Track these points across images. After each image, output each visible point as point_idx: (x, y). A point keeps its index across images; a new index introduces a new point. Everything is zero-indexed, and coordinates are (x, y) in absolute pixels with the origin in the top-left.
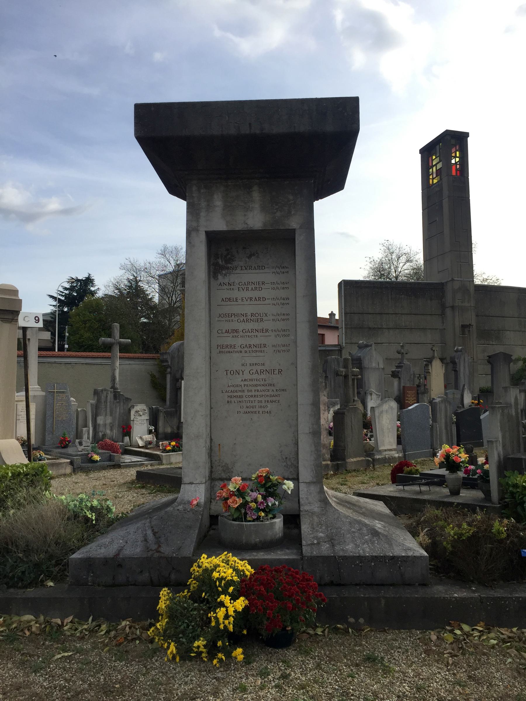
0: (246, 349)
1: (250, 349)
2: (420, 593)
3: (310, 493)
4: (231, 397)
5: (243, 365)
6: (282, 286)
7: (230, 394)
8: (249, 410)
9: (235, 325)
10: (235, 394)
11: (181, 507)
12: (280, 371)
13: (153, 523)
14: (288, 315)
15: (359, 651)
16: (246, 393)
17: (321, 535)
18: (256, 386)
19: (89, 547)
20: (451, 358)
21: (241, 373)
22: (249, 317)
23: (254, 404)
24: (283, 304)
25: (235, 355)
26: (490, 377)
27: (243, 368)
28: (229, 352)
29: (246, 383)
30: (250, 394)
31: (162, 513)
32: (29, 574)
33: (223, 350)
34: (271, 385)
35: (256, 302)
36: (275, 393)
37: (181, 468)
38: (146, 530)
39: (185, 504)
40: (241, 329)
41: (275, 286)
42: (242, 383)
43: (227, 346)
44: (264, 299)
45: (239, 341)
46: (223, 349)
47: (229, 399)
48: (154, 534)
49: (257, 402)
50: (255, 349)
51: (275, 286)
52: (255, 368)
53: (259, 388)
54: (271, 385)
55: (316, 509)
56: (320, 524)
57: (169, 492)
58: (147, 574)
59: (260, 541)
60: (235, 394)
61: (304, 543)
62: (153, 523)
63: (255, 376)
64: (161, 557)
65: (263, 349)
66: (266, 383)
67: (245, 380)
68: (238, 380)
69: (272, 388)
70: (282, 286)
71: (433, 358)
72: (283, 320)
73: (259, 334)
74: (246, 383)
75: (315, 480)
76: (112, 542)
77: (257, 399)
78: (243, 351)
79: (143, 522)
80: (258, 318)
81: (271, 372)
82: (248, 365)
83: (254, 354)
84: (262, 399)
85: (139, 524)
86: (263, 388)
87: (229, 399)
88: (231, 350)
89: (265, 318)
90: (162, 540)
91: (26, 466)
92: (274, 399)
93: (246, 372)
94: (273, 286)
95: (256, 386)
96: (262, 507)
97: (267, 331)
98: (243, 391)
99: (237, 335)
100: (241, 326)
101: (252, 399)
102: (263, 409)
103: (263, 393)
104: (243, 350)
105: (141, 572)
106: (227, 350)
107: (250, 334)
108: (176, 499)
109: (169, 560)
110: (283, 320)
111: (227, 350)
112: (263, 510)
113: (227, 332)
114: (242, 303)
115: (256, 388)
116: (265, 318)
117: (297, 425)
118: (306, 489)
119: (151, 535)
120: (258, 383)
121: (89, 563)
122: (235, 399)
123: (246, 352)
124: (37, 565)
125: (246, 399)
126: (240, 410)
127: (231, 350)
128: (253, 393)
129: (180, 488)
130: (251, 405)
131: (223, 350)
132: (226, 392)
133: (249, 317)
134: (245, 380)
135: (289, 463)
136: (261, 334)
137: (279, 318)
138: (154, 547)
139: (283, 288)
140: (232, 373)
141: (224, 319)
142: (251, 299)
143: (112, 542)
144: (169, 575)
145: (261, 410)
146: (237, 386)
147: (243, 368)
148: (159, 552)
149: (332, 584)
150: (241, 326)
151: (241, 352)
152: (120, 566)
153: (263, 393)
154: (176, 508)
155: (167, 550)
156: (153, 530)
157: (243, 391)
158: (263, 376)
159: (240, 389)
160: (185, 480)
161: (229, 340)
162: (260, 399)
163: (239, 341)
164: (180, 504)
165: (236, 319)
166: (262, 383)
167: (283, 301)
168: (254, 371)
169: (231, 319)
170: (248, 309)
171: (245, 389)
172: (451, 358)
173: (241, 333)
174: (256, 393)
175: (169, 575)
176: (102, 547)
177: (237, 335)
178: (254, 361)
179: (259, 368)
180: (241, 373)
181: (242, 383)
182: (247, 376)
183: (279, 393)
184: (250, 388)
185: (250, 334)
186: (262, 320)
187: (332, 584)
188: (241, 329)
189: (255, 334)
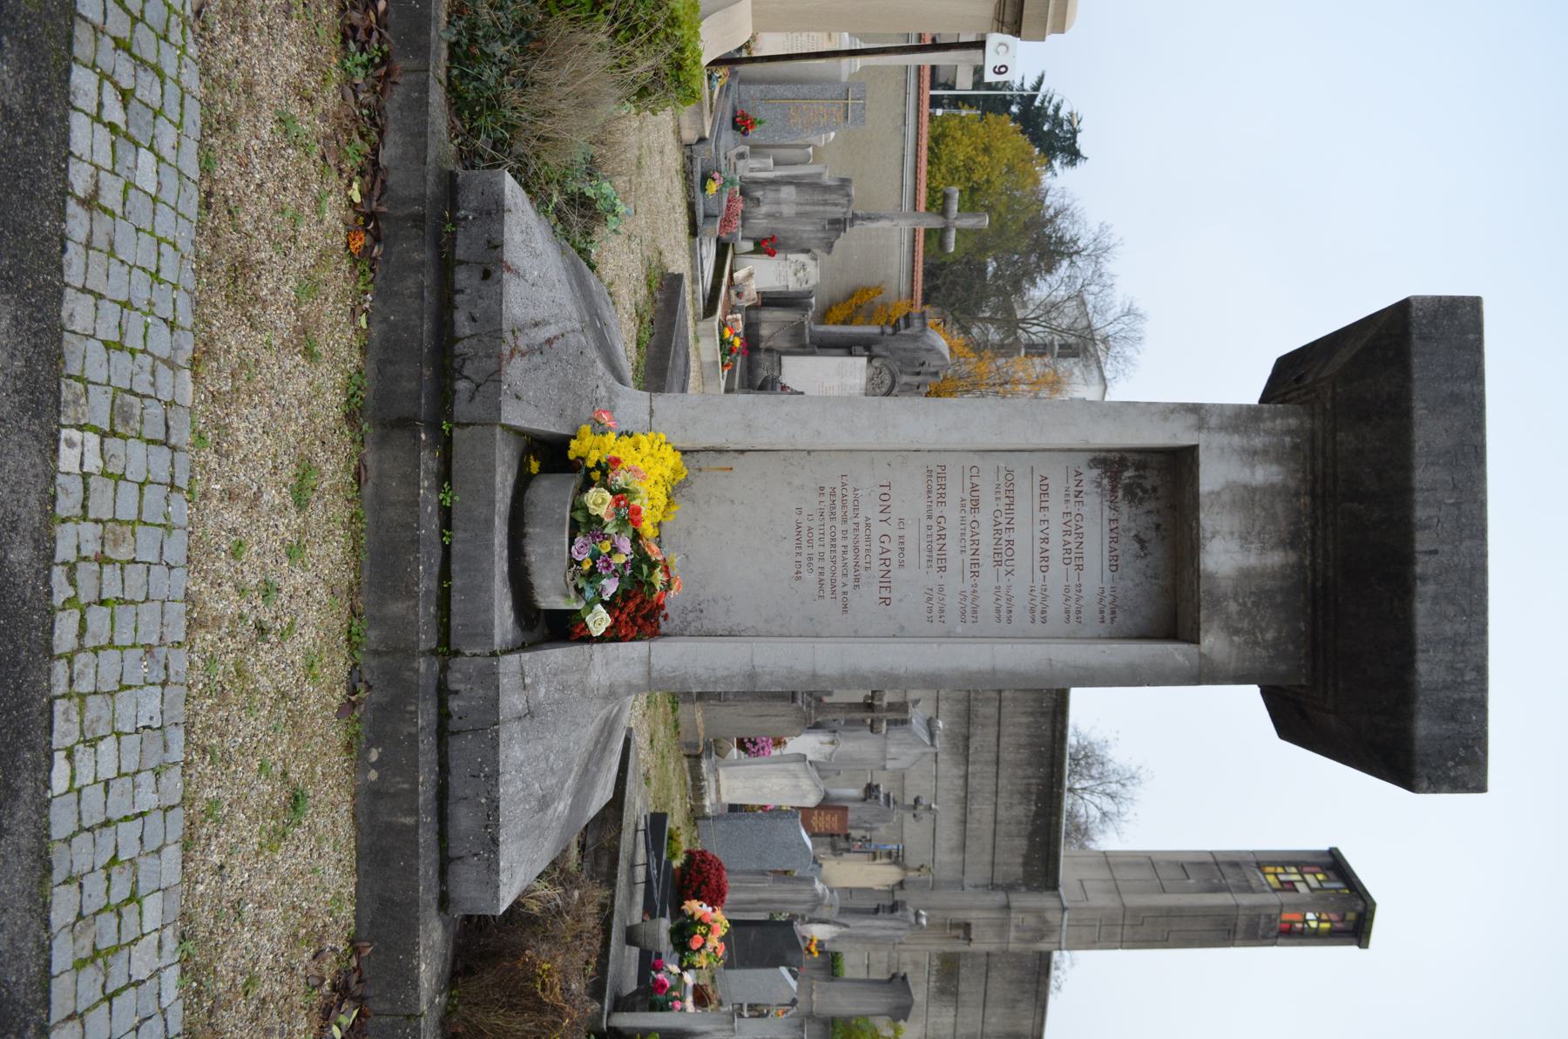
0: (936, 528)
1: (935, 537)
2: (427, 893)
3: (627, 665)
4: (833, 494)
6: (1073, 610)
7: (838, 492)
8: (804, 532)
9: (988, 503)
10: (838, 504)
11: (602, 392)
12: (885, 601)
13: (570, 336)
14: (1009, 620)
15: (314, 773)
16: (840, 527)
17: (542, 691)
18: (856, 548)
19: (528, 207)
20: (903, 903)
21: (884, 517)
22: (1005, 536)
23: (816, 543)
24: (1032, 610)
25: (922, 505)
26: (863, 976)
27: (894, 521)
28: (929, 492)
29: (862, 527)
30: (839, 535)
31: (593, 353)
32: (475, 88)
33: (934, 479)
34: (857, 579)
35: (1037, 551)
36: (839, 590)
37: (684, 390)
38: (557, 322)
39: (610, 399)
40: (978, 517)
41: (1072, 594)
42: (861, 520)
43: (942, 486)
45: (952, 514)
47: (827, 491)
48: (549, 342)
49: (822, 549)
50: (936, 547)
51: (1072, 594)
52: (894, 546)
53: (850, 555)
54: (857, 579)
55: (594, 677)
56: (564, 687)
57: (636, 370)
58: (468, 332)
59: (530, 564)
60: (838, 504)
61: (526, 656)
62: (570, 336)
63: (876, 548)
64: (499, 356)
65: (935, 564)
66: (862, 571)
67: (868, 526)
68: (869, 509)
69: (851, 584)
70: (1073, 610)
71: (905, 868)
72: (998, 611)
73: (967, 557)
74: (862, 527)
75: (654, 675)
76: (536, 255)
77: (827, 549)
78: (930, 522)
79: (575, 315)
80: (1003, 555)
81: (885, 583)
82: (901, 533)
83: (924, 545)
84: (827, 564)
85: (570, 308)
86: (851, 563)
87: (827, 491)
88: (934, 496)
90: (537, 359)
91: (696, 63)
92: (827, 587)
93: (885, 528)
94: (1073, 589)
95: (856, 548)
96: (600, 564)
97: (975, 574)
98: (845, 521)
99: (967, 508)
100: (985, 517)
101: (827, 539)
102: (805, 562)
103: (839, 564)
104: (932, 522)
105: (474, 319)
106: (935, 487)
107: (968, 537)
108: (621, 381)
109: (495, 376)
110: (998, 611)
111: (935, 487)
112: (593, 570)
113: (974, 488)
114: (1037, 520)
115: (850, 549)
116: (1002, 569)
117: (769, 635)
118: (635, 655)
119: (548, 335)
120: (862, 553)
121: (495, 210)
122: (827, 498)
123: (929, 528)
124: (493, 105)
125: (827, 527)
126: (805, 513)
127: (934, 496)
128: (839, 543)
129: (645, 389)
130: (816, 537)
131: (934, 479)
132: (844, 484)
133: (1005, 536)
134: (868, 526)
135: (691, 617)
136: (968, 562)
137: (1003, 602)
138: (522, 343)
139: (1067, 612)
141: (1002, 478)
142: (1045, 540)
143: (536, 255)
144: (467, 378)
145: (804, 559)
146: (856, 508)
147: (894, 521)
148: (512, 355)
149: (444, 715)
150: (985, 517)
151: (930, 517)
152: (486, 275)
153: (839, 564)
154: (600, 383)
155: (514, 371)
156: (556, 337)
157: (845, 521)
158: (876, 563)
159: (850, 514)
160: (660, 400)
161: (954, 493)
162: (827, 556)
163: (952, 514)
164: (609, 389)
165: (1002, 508)
166: (862, 562)
167: (1038, 609)
168: (886, 546)
169: (1002, 495)
170: (1023, 535)
171: (850, 526)
172: (903, 903)
173: (970, 518)
174: (839, 549)
175: (467, 378)
176: (526, 233)
177: (967, 508)
178: (910, 546)
179: (894, 556)
181: (861, 520)
182: (878, 529)
183: (840, 597)
184: (850, 536)
185: (968, 537)
186: (998, 563)
187: (444, 715)
188: (978, 517)
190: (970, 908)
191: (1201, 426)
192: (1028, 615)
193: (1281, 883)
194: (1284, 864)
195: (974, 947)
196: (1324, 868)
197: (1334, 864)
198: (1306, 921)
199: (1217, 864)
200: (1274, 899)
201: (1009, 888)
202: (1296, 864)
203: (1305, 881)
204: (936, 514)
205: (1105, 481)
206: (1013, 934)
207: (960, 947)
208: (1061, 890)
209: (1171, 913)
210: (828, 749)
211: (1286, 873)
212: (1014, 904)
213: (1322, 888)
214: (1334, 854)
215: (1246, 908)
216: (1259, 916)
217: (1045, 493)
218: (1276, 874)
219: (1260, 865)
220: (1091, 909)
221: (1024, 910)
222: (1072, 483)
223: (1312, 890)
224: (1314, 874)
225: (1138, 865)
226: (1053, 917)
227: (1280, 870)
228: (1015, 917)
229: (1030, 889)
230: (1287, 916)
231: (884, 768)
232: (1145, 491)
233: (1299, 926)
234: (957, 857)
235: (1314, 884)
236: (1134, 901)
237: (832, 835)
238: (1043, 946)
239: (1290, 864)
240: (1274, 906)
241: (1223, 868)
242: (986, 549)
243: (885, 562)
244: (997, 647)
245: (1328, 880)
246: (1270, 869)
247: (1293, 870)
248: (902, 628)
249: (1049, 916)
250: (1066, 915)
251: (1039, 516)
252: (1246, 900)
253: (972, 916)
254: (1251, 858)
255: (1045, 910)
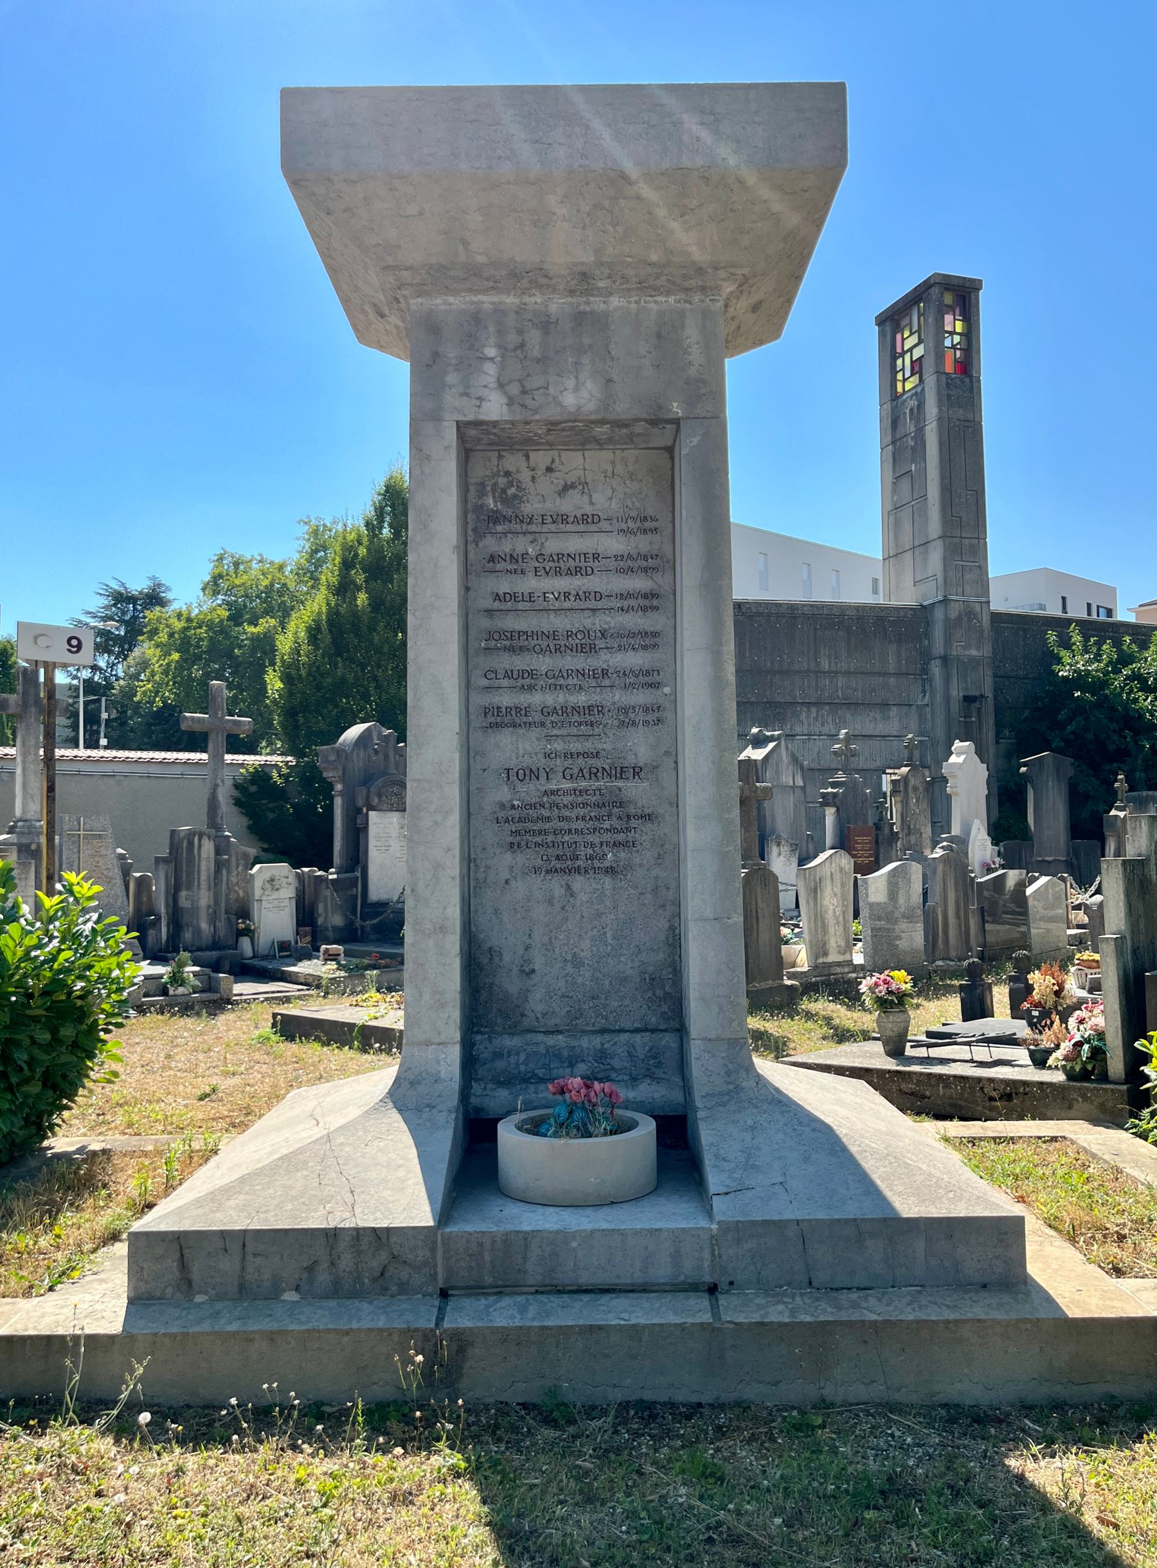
0: (554, 718)
5: (547, 755)
10: (530, 826)
21: (543, 775)
44: (599, 596)
46: (499, 719)
67: (553, 792)
89: (600, 644)
92: (621, 837)
98: (549, 819)
116: (600, 644)
132: (507, 821)
140: (521, 776)
142: (567, 595)
150: (543, 663)
151: (543, 724)
157: (549, 819)
168: (576, 771)
178: (576, 746)
180: (543, 775)
188: (544, 669)
189: (575, 681)
190: (947, 698)
191: (435, 417)
192: (649, 614)
193: (912, 374)
194: (894, 372)
195: (989, 694)
196: (897, 328)
197: (892, 321)
198: (953, 347)
199: (894, 442)
200: (931, 380)
201: (926, 657)
202: (894, 357)
203: (911, 350)
204: (538, 717)
205: (499, 528)
206: (974, 652)
207: (989, 706)
208: (925, 603)
209: (947, 490)
210: (785, 849)
211: (903, 369)
212: (942, 653)
213: (919, 331)
214: (881, 321)
215: (940, 410)
216: (949, 396)
217: (514, 597)
218: (905, 380)
219: (895, 397)
220: (945, 570)
221: (948, 641)
222: (501, 566)
223: (920, 342)
224: (903, 340)
225: (897, 524)
226: (954, 611)
227: (900, 376)
228: (957, 650)
229: (927, 635)
230: (949, 368)
231: (803, 788)
232: (510, 484)
233: (958, 353)
234: (894, 711)
235: (914, 339)
236: (934, 526)
237: (877, 842)
238: (986, 620)
239: (894, 365)
240: (938, 380)
241: (898, 436)
242: (577, 662)
243: (594, 774)
244: (686, 645)
245: (911, 325)
246: (900, 389)
247: (899, 362)
248: (667, 753)
249: (953, 614)
250: (952, 597)
251: (540, 603)
252: (932, 409)
253: (956, 693)
254: (888, 406)
255: (947, 620)
